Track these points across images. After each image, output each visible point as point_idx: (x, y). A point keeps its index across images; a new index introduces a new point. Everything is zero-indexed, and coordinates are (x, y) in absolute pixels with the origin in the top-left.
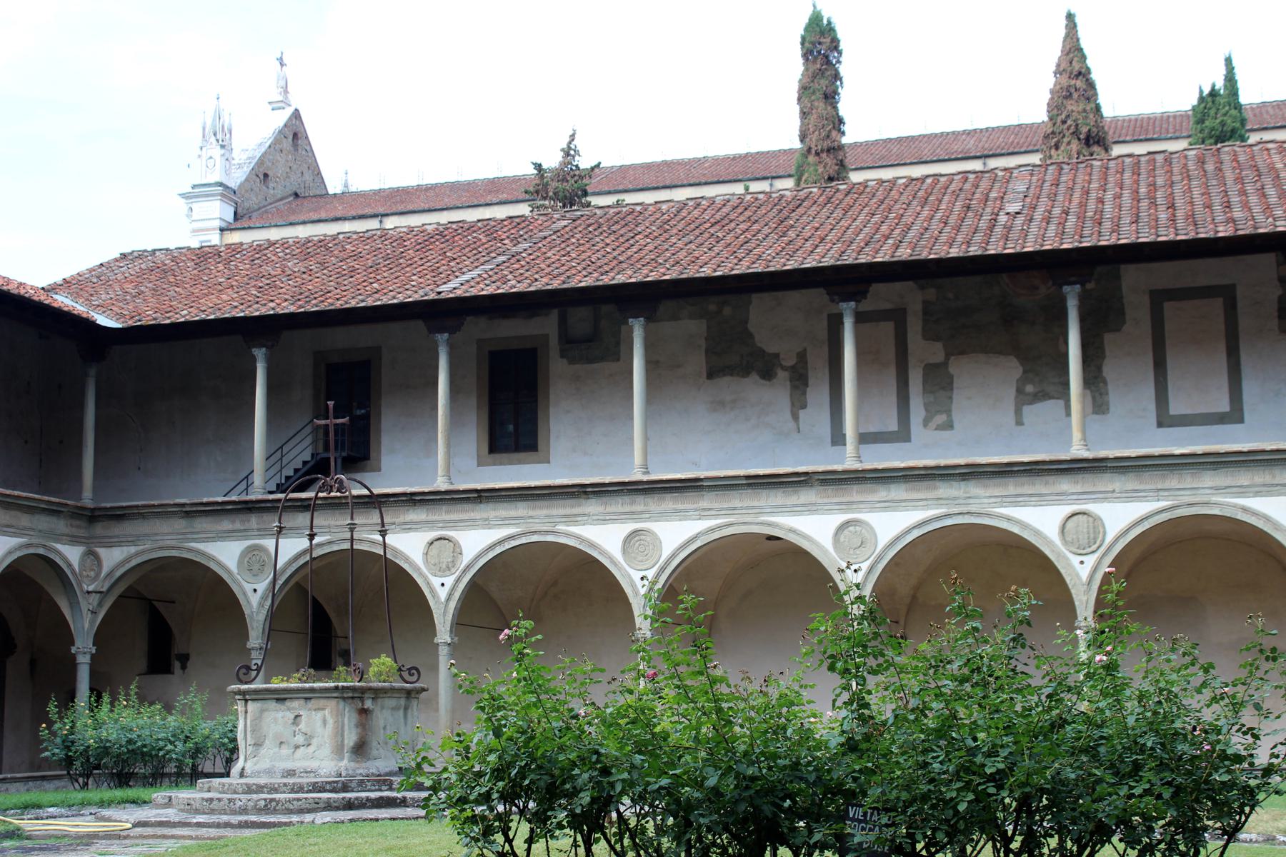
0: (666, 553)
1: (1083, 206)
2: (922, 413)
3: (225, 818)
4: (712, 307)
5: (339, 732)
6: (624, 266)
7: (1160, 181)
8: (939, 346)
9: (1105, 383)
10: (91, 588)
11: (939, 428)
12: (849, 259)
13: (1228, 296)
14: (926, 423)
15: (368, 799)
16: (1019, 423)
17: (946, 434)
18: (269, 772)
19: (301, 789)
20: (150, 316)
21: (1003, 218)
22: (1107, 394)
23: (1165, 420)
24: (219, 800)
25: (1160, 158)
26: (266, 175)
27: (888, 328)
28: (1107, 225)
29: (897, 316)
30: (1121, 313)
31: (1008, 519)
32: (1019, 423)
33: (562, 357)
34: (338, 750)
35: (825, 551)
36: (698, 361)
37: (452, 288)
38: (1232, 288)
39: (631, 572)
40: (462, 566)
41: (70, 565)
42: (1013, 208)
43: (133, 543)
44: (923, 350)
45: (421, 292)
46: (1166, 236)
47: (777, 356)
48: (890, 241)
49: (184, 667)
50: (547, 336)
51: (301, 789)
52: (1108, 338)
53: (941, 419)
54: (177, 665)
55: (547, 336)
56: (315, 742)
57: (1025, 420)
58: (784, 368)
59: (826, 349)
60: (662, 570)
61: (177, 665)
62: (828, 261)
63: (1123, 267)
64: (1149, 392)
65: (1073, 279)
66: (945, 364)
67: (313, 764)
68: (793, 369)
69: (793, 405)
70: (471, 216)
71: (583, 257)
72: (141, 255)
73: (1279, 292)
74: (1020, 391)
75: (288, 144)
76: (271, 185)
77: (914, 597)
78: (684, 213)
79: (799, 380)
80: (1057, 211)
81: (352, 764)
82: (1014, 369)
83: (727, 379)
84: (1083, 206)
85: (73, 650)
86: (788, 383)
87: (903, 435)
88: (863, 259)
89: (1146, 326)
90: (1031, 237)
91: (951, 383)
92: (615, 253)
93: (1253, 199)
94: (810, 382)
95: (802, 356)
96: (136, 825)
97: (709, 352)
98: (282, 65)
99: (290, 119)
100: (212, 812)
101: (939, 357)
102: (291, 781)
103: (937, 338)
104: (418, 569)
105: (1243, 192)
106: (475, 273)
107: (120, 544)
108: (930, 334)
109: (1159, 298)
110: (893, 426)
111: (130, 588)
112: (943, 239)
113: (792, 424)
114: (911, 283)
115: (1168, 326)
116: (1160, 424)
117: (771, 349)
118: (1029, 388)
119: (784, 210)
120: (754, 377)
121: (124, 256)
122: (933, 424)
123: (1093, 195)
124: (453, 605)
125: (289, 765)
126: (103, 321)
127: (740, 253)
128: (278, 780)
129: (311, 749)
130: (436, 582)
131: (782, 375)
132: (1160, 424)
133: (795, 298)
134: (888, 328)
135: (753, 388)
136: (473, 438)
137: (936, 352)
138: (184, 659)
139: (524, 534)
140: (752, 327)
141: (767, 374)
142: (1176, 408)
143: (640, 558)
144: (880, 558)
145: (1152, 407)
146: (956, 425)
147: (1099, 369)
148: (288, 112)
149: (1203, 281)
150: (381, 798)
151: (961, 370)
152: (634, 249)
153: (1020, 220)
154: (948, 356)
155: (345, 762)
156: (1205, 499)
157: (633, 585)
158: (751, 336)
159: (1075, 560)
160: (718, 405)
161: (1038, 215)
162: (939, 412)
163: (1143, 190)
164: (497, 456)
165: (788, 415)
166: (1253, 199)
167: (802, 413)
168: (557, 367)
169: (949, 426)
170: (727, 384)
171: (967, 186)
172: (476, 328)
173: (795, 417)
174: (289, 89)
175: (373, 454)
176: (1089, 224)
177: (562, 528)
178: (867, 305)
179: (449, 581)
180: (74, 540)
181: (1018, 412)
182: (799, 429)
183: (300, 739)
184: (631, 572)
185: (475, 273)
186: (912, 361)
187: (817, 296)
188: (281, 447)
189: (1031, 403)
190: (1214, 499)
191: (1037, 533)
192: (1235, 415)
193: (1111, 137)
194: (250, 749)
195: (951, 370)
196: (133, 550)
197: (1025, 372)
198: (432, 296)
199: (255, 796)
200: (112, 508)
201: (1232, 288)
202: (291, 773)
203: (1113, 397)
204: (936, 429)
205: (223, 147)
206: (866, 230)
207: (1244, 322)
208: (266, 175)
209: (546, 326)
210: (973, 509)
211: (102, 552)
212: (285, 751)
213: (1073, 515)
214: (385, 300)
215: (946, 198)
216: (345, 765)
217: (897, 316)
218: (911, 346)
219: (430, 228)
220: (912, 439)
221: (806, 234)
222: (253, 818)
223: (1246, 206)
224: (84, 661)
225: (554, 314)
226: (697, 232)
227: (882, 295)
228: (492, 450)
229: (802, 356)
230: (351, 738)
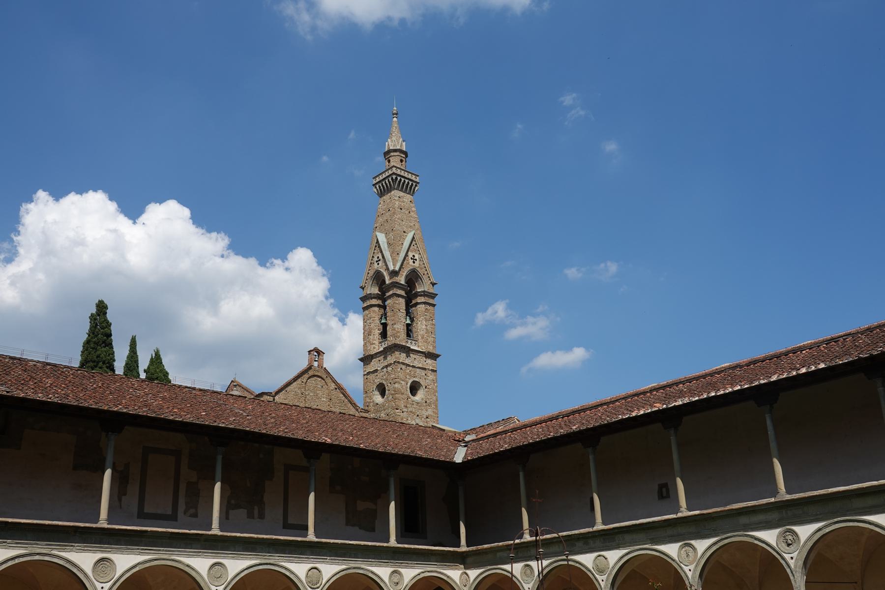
0: (118, 574)
11: (192, 516)
17: (194, 519)
31: (286, 569)
39: (96, 583)
53: (192, 511)
64: (281, 512)
110: (169, 512)
116: (284, 527)
118: (233, 502)
132: (284, 527)
142: (291, 521)
143: (102, 575)
144: (229, 583)
167: (124, 498)
169: (195, 515)
173: (120, 500)
182: (121, 506)
184: (96, 583)
191: (297, 576)
204: (189, 516)
213: (312, 568)
220: (179, 519)
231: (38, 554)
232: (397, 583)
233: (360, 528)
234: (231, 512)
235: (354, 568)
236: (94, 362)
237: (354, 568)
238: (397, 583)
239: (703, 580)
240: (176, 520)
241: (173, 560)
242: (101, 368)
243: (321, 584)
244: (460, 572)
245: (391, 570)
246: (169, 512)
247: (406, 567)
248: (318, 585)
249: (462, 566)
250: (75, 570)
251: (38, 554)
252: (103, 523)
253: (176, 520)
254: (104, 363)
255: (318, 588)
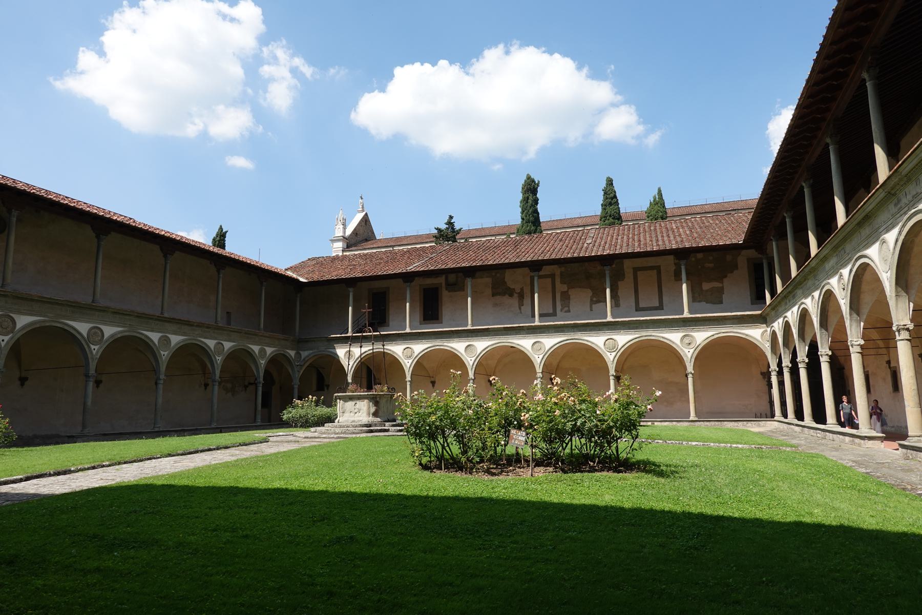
0: (479, 352)
1: (611, 241)
2: (561, 307)
3: (332, 436)
4: (494, 274)
5: (369, 408)
6: (465, 261)
7: (636, 233)
8: (565, 286)
9: (619, 297)
10: (298, 364)
11: (565, 312)
12: (535, 258)
13: (658, 269)
14: (561, 311)
15: (377, 429)
16: (591, 310)
18: (347, 421)
19: (356, 427)
20: (316, 277)
21: (586, 245)
22: (619, 301)
23: (638, 309)
24: (331, 430)
25: (636, 226)
26: (357, 234)
27: (549, 280)
28: (618, 247)
29: (552, 276)
30: (624, 275)
32: (591, 310)
33: (446, 290)
34: (369, 414)
35: (528, 350)
36: (489, 291)
37: (411, 268)
38: (660, 266)
39: (468, 358)
40: (414, 357)
41: (291, 357)
42: (589, 242)
43: (311, 350)
44: (561, 287)
45: (401, 270)
46: (637, 250)
47: (514, 289)
48: (549, 253)
49: (328, 389)
50: (441, 284)
51: (356, 427)
52: (619, 283)
53: (566, 309)
54: (326, 388)
55: (442, 283)
56: (361, 411)
57: (593, 310)
58: (516, 293)
59: (530, 287)
60: (477, 357)
61: (326, 388)
62: (529, 259)
63: (624, 260)
65: (607, 264)
66: (567, 291)
67: (361, 418)
68: (519, 293)
69: (519, 304)
70: (418, 246)
71: (453, 258)
72: (314, 259)
73: (674, 268)
74: (591, 300)
75: (363, 224)
76: (358, 236)
77: (558, 365)
78: (485, 244)
79: (521, 296)
80: (603, 243)
81: (373, 418)
82: (589, 293)
83: (499, 296)
84: (611, 241)
85: (293, 384)
86: (518, 298)
87: (554, 314)
88: (540, 258)
89: (632, 277)
90: (594, 251)
91: (569, 298)
92: (462, 257)
93: (666, 238)
94: (525, 297)
95: (522, 289)
96: (305, 438)
97: (493, 288)
98: (362, 198)
99: (364, 216)
100: (329, 434)
101: (566, 289)
102: (353, 424)
103: (565, 283)
104: (400, 357)
105: (662, 236)
106: (419, 263)
107: (307, 350)
108: (562, 282)
109: (636, 270)
110: (551, 311)
111: (310, 364)
112: (566, 252)
113: (519, 311)
114: (556, 266)
115: (639, 279)
116: (636, 310)
117: (512, 287)
118: (594, 299)
119: (516, 244)
120: (507, 296)
121: (309, 259)
122: (564, 310)
123: (615, 237)
124: (411, 369)
125: (352, 419)
126: (302, 280)
127: (502, 257)
128: (349, 424)
129: (360, 414)
130: (406, 361)
131: (516, 295)
132: (636, 310)
133: (519, 271)
134: (549, 280)
135: (506, 300)
136: (418, 316)
137: (565, 288)
138: (328, 386)
139: (434, 346)
140: (506, 280)
141: (511, 295)
142: (642, 305)
144: (546, 353)
145: (634, 304)
146: (571, 310)
147: (617, 293)
148: (364, 213)
149: (650, 265)
150: (382, 429)
151: (571, 292)
152: (469, 255)
153: (591, 245)
154: (568, 289)
155: (371, 418)
156: (650, 334)
157: (468, 362)
158: (506, 283)
159: (608, 354)
160: (495, 305)
161: (596, 244)
162: (565, 307)
163: (630, 236)
164: (426, 322)
165: (518, 308)
166: (666, 238)
167: (522, 307)
168: (445, 294)
169: (569, 311)
170: (498, 299)
171: (575, 235)
172: (418, 281)
174: (364, 206)
175: (387, 322)
176: (612, 247)
177: (445, 344)
178: (541, 273)
179: (410, 361)
180: (292, 349)
181: (591, 307)
183: (356, 411)
184: (468, 358)
185: (419, 263)
186: (557, 290)
187: (526, 270)
188: (358, 319)
189: (595, 304)
190: (653, 334)
191: (596, 345)
192: (660, 308)
193: (624, 218)
194: (341, 414)
195: (570, 293)
196: (311, 351)
197: (593, 294)
198: (405, 271)
199: (342, 429)
200: (306, 339)
201: (660, 266)
202: (353, 421)
203: (621, 302)
205: (343, 225)
206: (542, 249)
207: (663, 277)
208: (357, 234)
209: (441, 280)
210: (576, 337)
211: (301, 352)
212: (352, 414)
214: (390, 272)
215: (568, 239)
216: (371, 419)
217: (552, 276)
218: (557, 286)
219: (405, 250)
221: (523, 251)
222: (342, 435)
223: (663, 241)
224: (296, 387)
225: (444, 277)
226: (489, 250)
227: (546, 270)
228: (424, 320)
229: (522, 289)
230: (373, 409)
231: (438, 346)
232: (690, 344)
233: (706, 303)
234: (593, 305)
235: (646, 336)
236: (605, 217)
237: (646, 336)
238: (690, 344)
239: (831, 330)
240: (556, 316)
241: (509, 342)
242: (608, 220)
243: (617, 349)
244: (761, 330)
245: (681, 335)
246: (551, 311)
247: (698, 331)
248: (615, 350)
249: (765, 325)
250: (456, 352)
251: (438, 346)
252: (469, 327)
253: (556, 316)
254: (610, 216)
255: (614, 351)
